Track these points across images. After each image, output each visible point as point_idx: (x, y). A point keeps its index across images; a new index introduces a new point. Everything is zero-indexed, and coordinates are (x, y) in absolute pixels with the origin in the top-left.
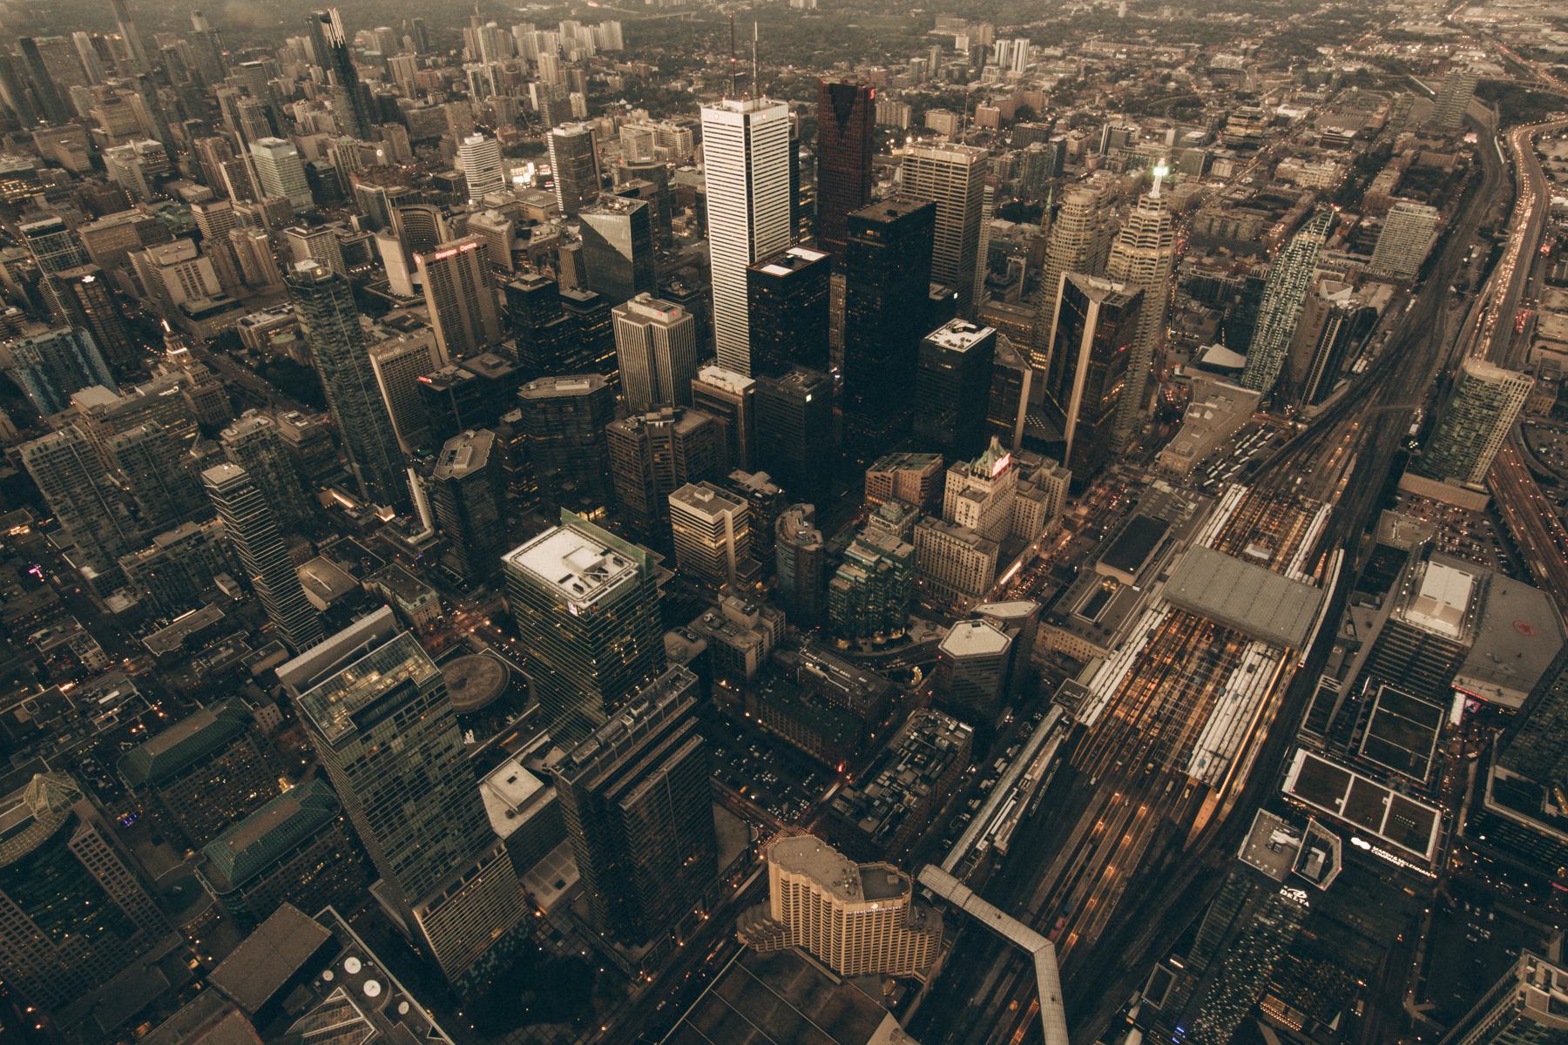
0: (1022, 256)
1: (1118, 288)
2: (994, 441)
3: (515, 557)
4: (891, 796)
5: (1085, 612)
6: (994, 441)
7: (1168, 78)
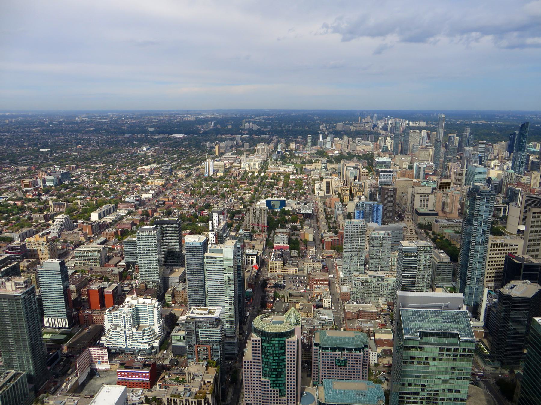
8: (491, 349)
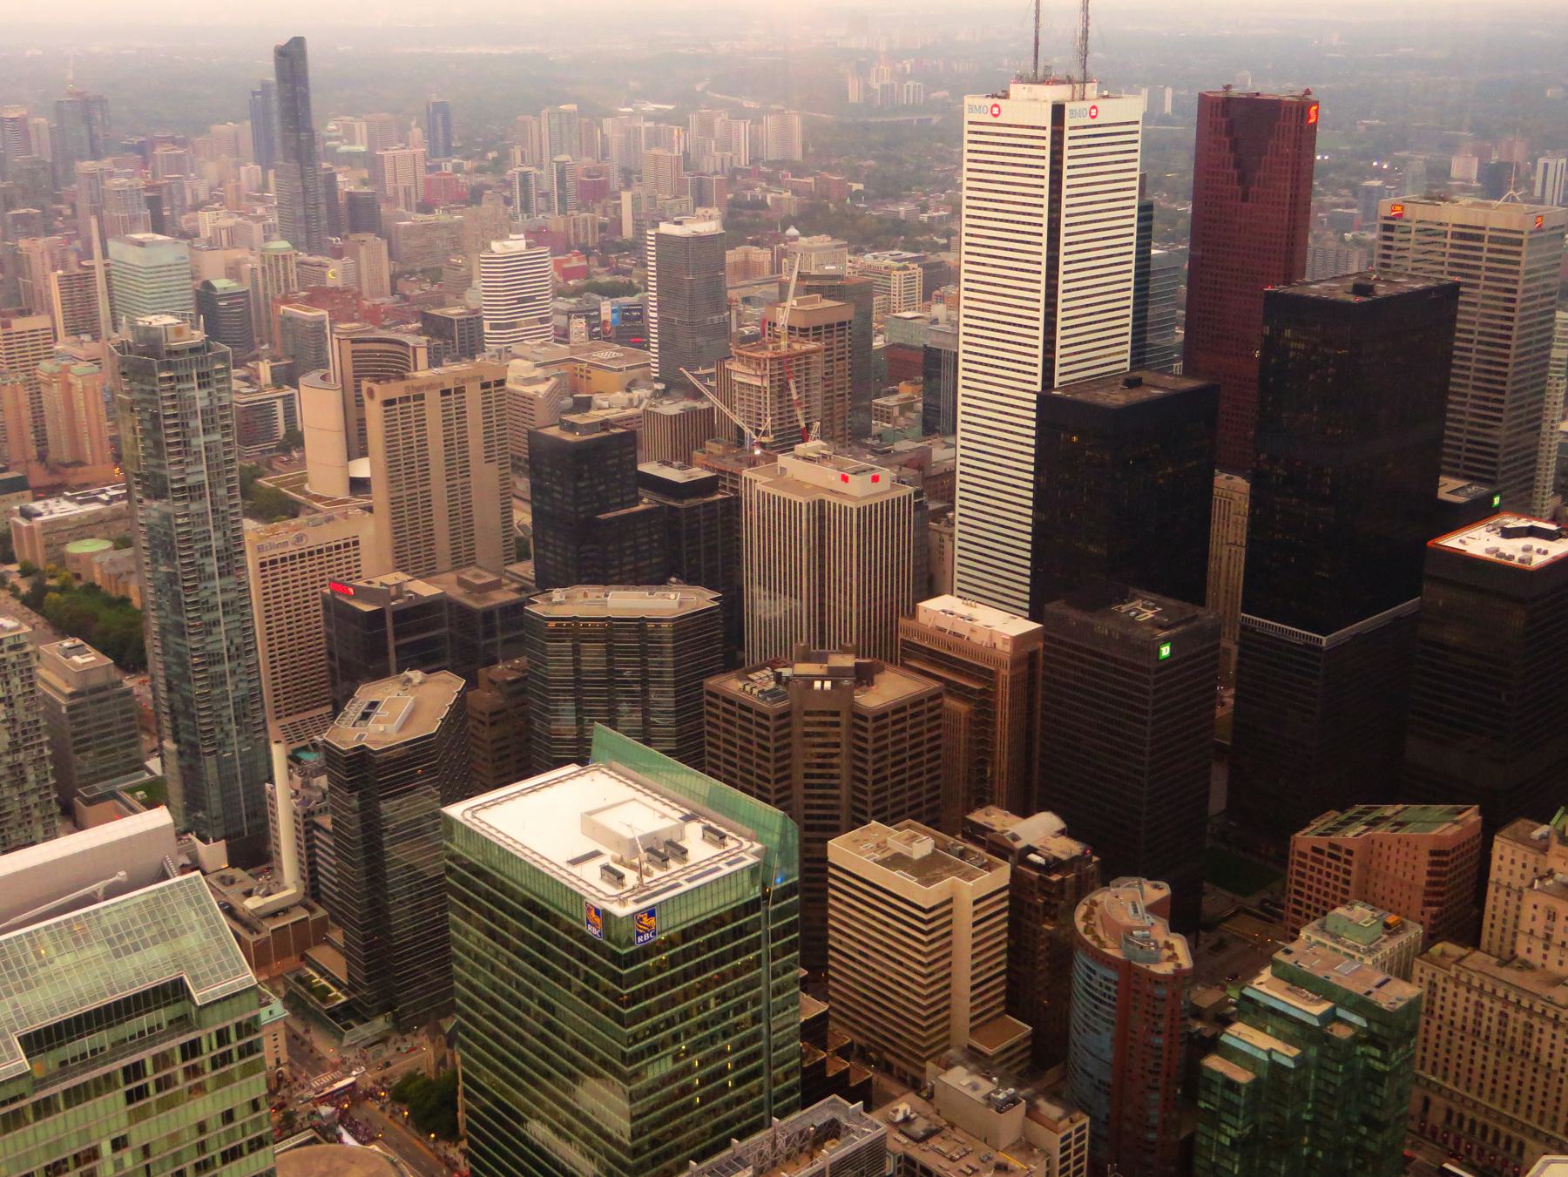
8: (349, 975)
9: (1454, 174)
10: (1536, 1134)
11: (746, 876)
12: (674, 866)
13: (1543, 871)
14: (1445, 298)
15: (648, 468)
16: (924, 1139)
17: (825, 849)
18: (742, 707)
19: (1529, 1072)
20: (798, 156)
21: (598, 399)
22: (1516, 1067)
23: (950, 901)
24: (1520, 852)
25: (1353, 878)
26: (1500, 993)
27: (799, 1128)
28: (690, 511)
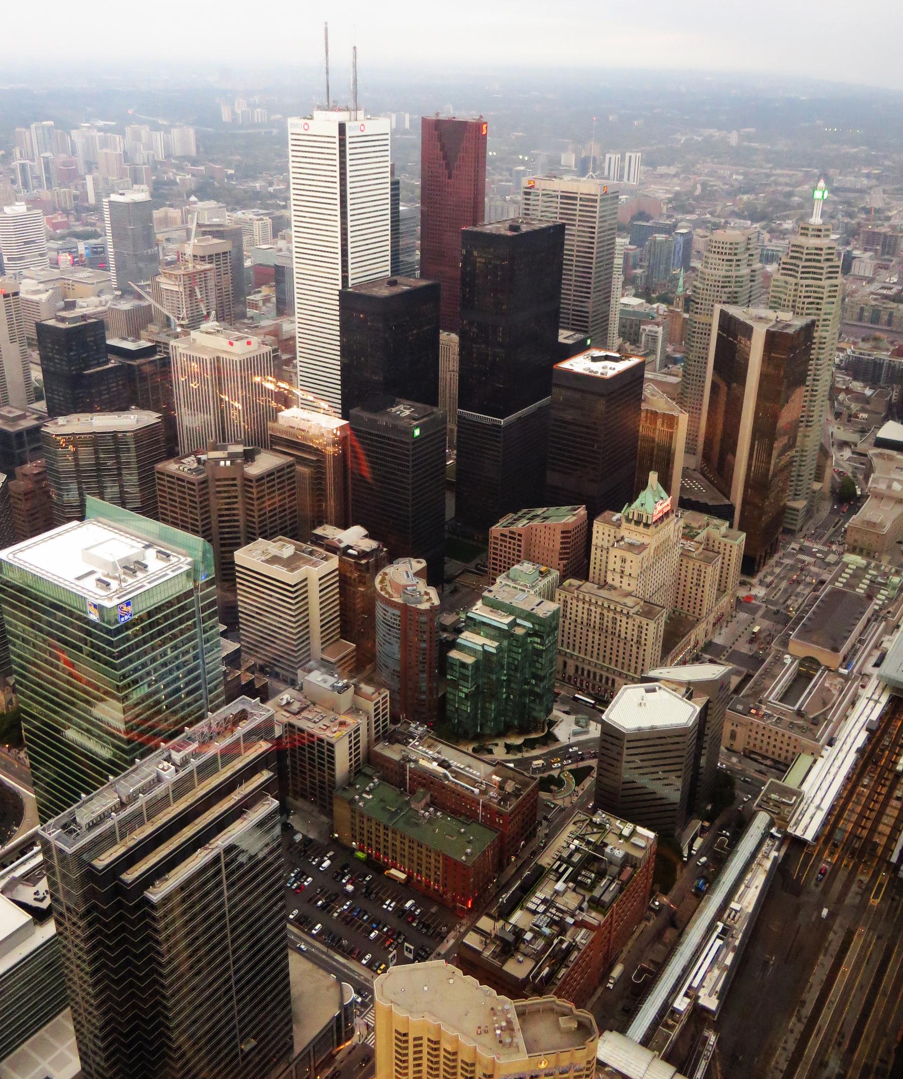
0: (658, 325)
1: (786, 316)
2: (653, 477)
3: (13, 553)
4: (549, 925)
5: (784, 698)
6: (653, 477)
7: (790, 195)
9: (563, 163)
10: (620, 674)
11: (184, 577)
12: (140, 575)
13: (618, 538)
14: (560, 230)
15: (113, 342)
16: (299, 713)
17: (233, 557)
18: (179, 479)
19: (615, 643)
20: (193, 152)
21: (80, 302)
22: (609, 641)
23: (306, 579)
24: (607, 529)
25: (522, 549)
26: (600, 603)
27: (223, 716)
28: (139, 366)
